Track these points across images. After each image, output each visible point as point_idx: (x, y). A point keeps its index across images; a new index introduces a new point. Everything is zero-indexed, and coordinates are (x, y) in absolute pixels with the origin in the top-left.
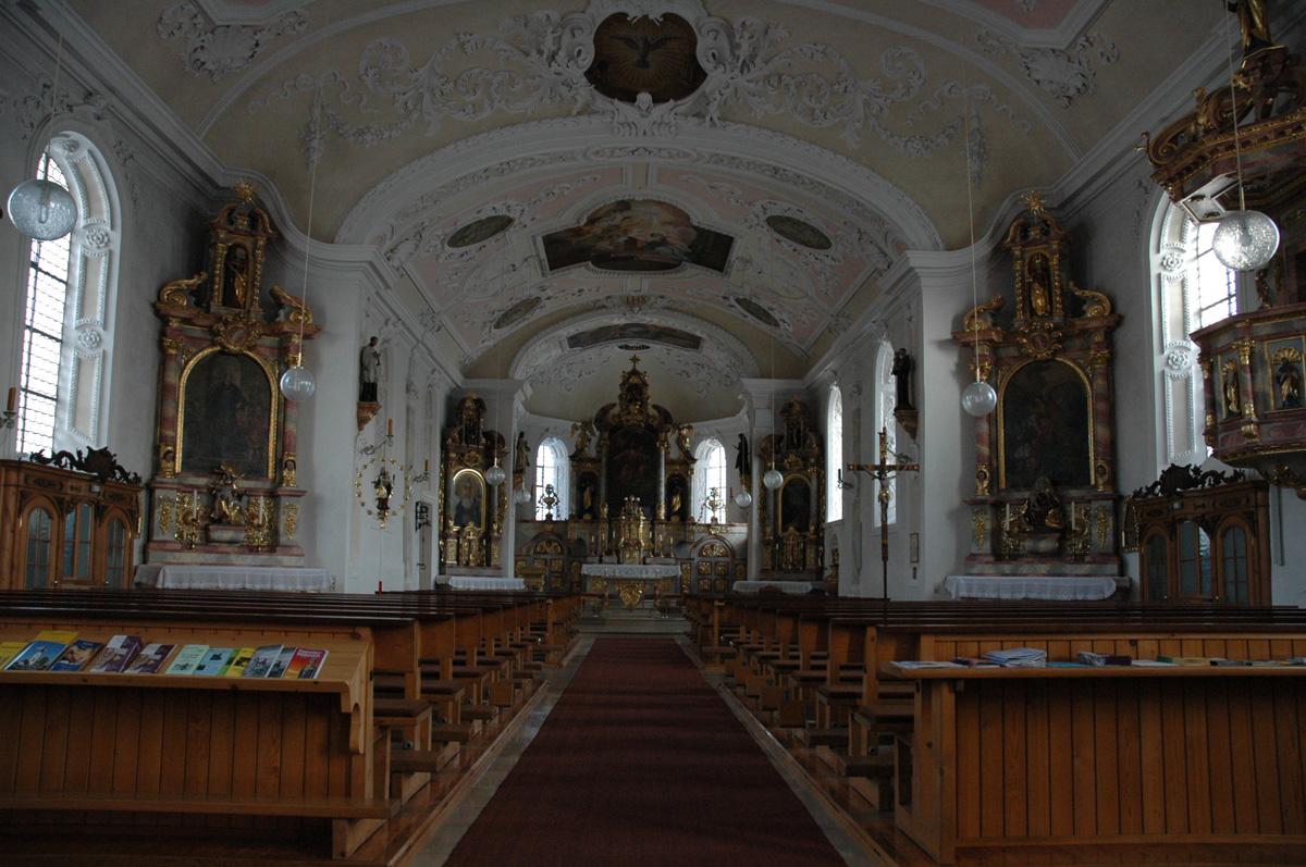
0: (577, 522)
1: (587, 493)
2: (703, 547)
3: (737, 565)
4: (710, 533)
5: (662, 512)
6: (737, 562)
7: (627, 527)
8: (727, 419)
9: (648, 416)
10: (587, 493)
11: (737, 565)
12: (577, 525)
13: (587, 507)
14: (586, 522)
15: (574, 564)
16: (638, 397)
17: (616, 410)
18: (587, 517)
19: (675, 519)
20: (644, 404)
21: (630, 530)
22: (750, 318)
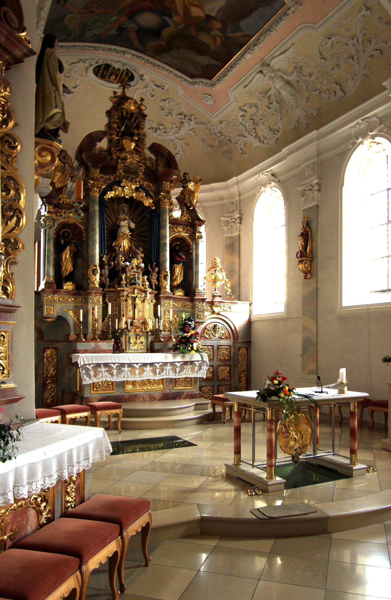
0: (54, 292)
1: (67, 255)
2: (205, 328)
3: (239, 348)
4: (213, 312)
5: (167, 285)
6: (239, 345)
7: (130, 302)
8: (214, 185)
9: (145, 159)
10: (67, 255)
11: (239, 348)
12: (56, 297)
13: (66, 273)
14: (68, 292)
15: (48, 352)
16: (136, 132)
17: (103, 144)
18: (68, 286)
19: (179, 293)
20: (140, 143)
21: (134, 306)
22: (234, 70)
